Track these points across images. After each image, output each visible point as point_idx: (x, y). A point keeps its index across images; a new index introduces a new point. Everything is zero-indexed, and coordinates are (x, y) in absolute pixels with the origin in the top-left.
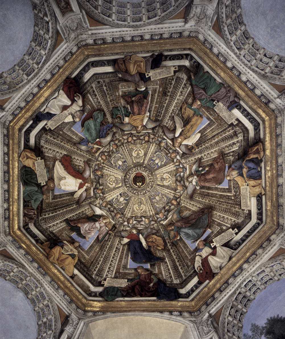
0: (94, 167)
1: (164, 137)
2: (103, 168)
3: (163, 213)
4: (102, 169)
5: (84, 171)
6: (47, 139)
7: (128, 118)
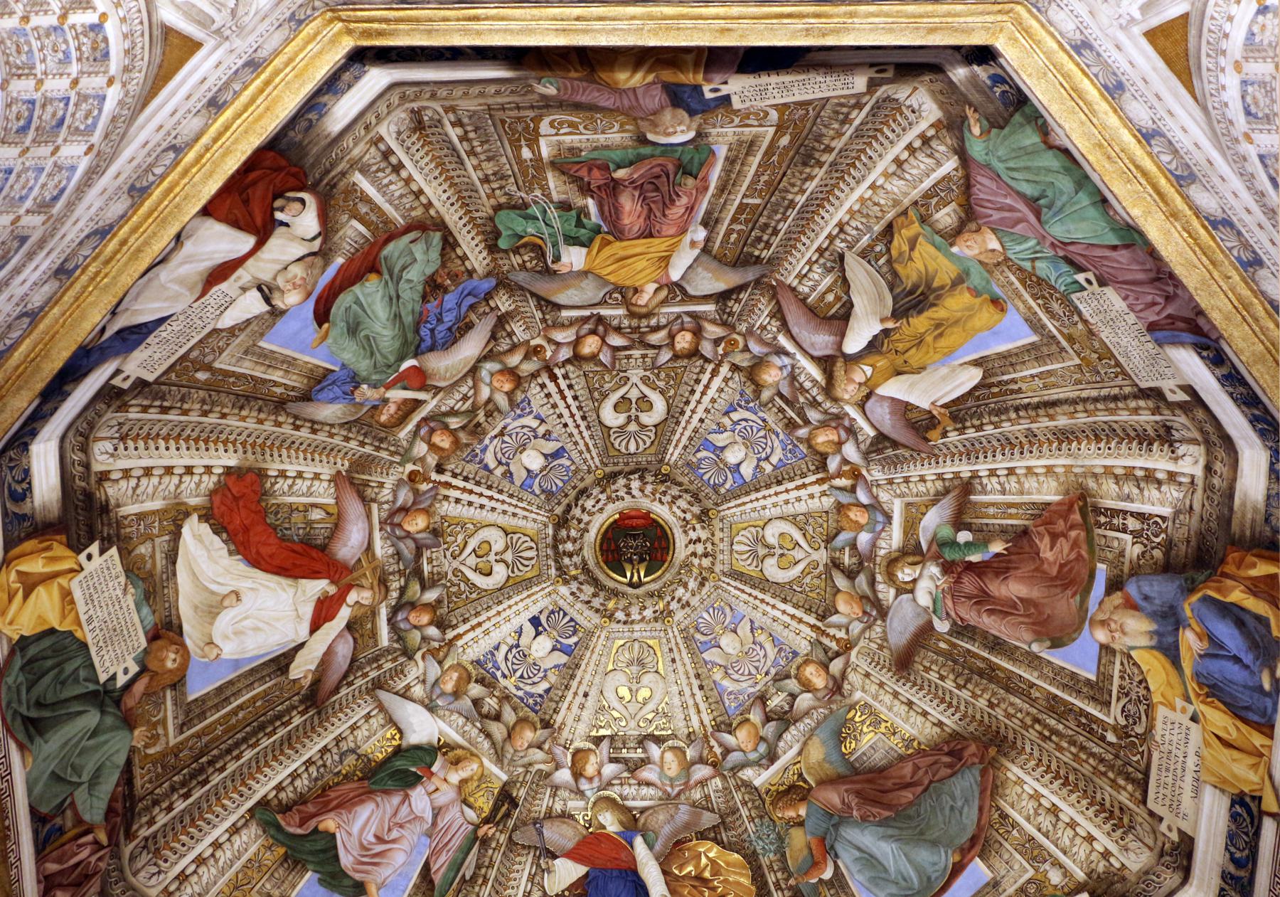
0: (390, 498)
1: (783, 341)
3: (754, 725)
4: (435, 497)
5: (337, 523)
6: (125, 428)
7: (584, 250)
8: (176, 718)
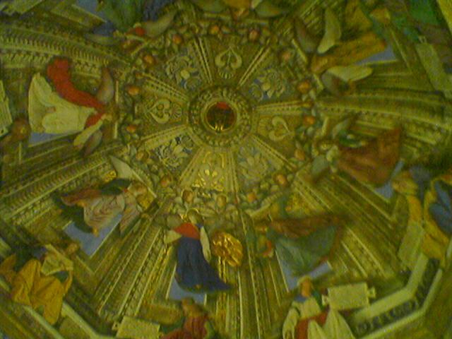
1: (293, 42)
2: (143, 82)
3: (254, 194)
4: (143, 83)
5: (101, 86)
6: (10, 32)
8: (22, 153)
